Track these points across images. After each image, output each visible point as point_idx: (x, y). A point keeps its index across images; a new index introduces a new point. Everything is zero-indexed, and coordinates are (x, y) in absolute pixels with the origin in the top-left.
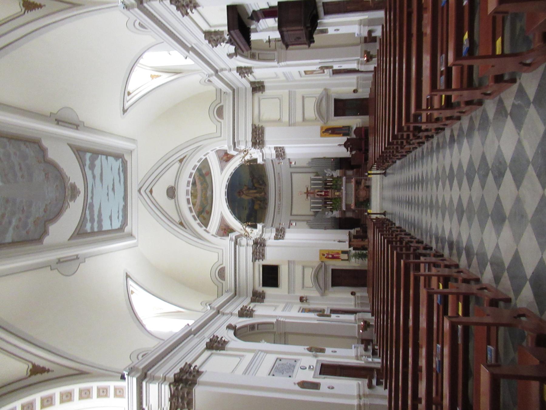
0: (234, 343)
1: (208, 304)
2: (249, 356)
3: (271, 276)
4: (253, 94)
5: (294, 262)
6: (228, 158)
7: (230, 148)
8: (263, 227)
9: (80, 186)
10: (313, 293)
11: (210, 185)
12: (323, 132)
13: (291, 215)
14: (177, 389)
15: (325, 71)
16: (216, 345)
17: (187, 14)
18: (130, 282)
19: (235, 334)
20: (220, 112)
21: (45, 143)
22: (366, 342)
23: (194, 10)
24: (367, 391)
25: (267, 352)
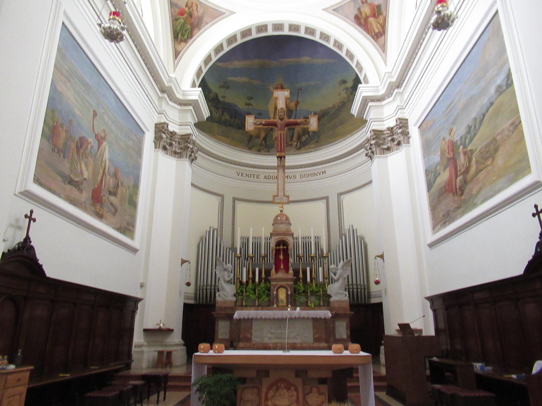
6: (367, 18)
8: (194, 104)
13: (235, 199)
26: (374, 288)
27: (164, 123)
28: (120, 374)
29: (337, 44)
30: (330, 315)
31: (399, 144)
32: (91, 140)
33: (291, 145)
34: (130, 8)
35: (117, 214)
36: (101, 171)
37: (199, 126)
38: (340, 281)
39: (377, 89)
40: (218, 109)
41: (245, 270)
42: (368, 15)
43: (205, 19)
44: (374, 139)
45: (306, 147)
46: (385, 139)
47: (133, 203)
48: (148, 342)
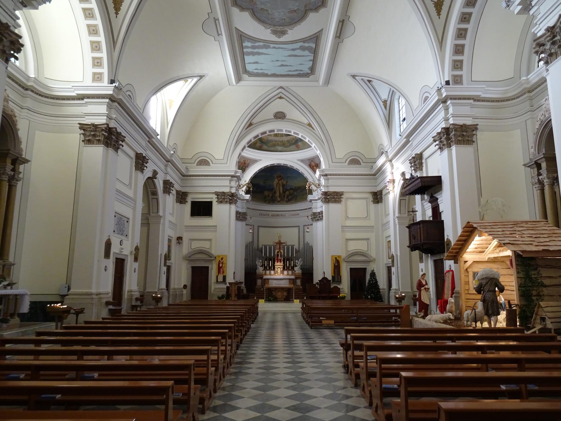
0: (141, 179)
1: (174, 150)
2: (130, 193)
3: (202, 209)
4: (371, 192)
5: (216, 231)
7: (323, 171)
8: (247, 200)
9: (284, 39)
10: (185, 249)
11: (288, 149)
12: (336, 258)
13: (258, 227)
14: (103, 130)
15: (390, 260)
16: (140, 162)
17: (435, 141)
18: (195, 80)
19: (149, 178)
20: (355, 162)
21: (322, 11)
22: (141, 299)
23: (437, 147)
24: (104, 301)
25: (134, 209)
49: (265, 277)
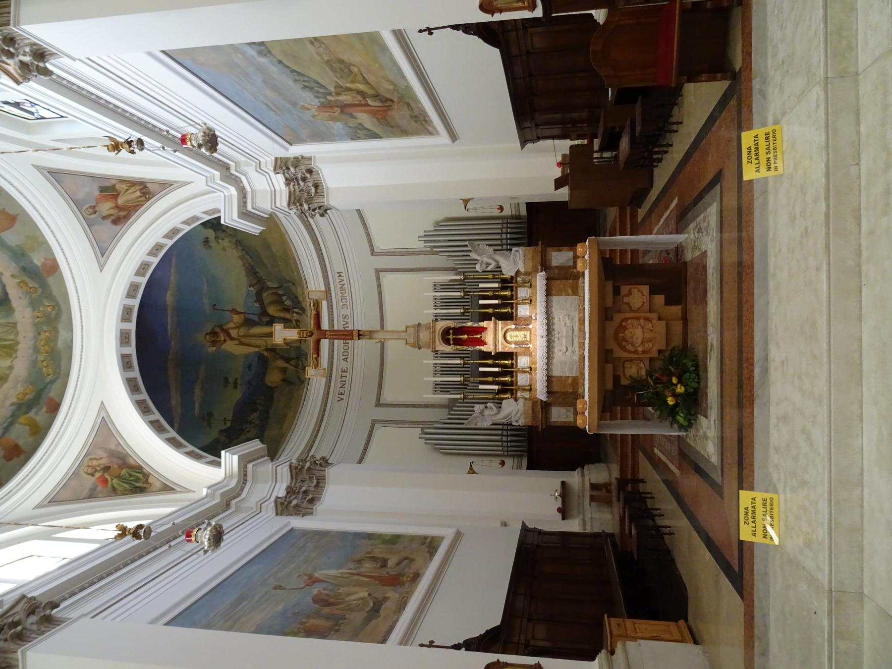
6: (117, 207)
8: (244, 461)
11: (63, 307)
13: (378, 404)
26: (507, 212)
27: (276, 502)
28: (618, 543)
29: (155, 252)
30: (544, 273)
31: (310, 171)
32: (315, 590)
33: (297, 321)
34: (50, 582)
35: (411, 557)
36: (356, 577)
37: (273, 454)
38: (498, 258)
39: (227, 199)
40: (243, 430)
41: (481, 387)
42: (112, 205)
43: (112, 446)
44: (301, 205)
45: (300, 299)
46: (302, 190)
47: (395, 539)
48: (579, 513)
49: (541, 394)
